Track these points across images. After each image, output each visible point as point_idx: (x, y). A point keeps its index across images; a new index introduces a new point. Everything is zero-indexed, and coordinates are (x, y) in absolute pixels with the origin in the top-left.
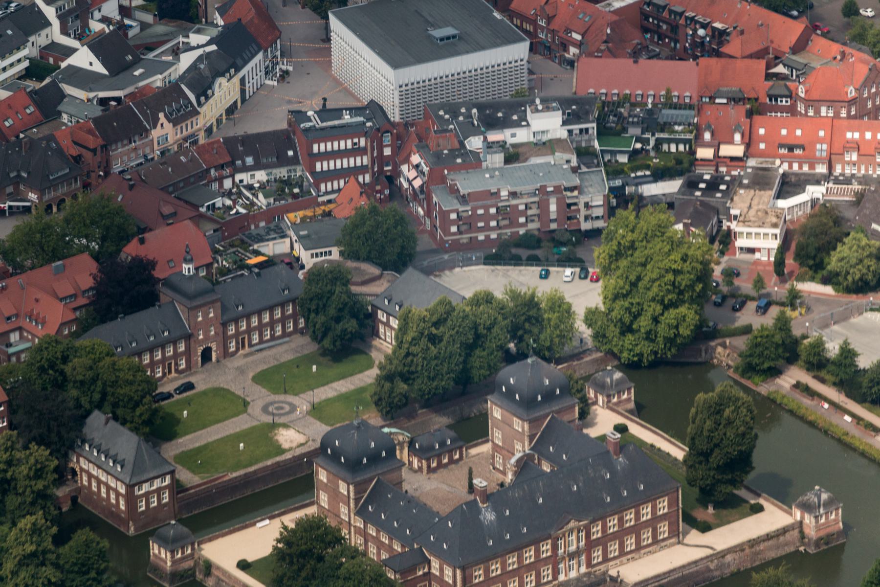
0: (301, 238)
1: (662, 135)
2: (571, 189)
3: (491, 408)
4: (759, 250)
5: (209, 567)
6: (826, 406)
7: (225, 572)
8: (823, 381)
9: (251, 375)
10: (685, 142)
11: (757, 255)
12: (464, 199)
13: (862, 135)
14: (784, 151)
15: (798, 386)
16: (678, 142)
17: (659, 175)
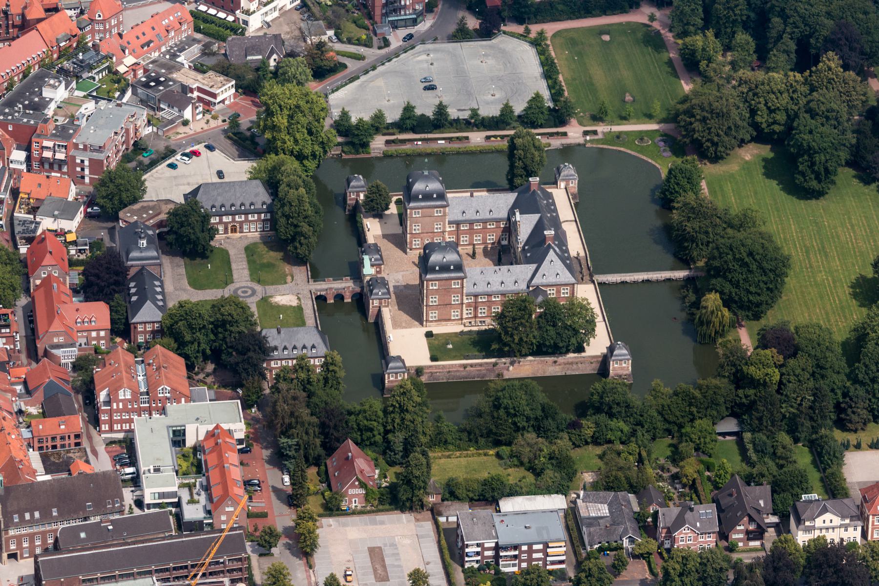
0: (56, 217)
1: (96, 71)
2: (133, 116)
3: (411, 213)
4: (226, 99)
5: (419, 371)
6: (420, 143)
7: (431, 367)
8: (393, 134)
9: (189, 288)
10: (104, 69)
11: (227, 102)
12: (100, 149)
13: (169, 20)
14: (146, 48)
15: (388, 142)
16: (101, 71)
17: (123, 92)
